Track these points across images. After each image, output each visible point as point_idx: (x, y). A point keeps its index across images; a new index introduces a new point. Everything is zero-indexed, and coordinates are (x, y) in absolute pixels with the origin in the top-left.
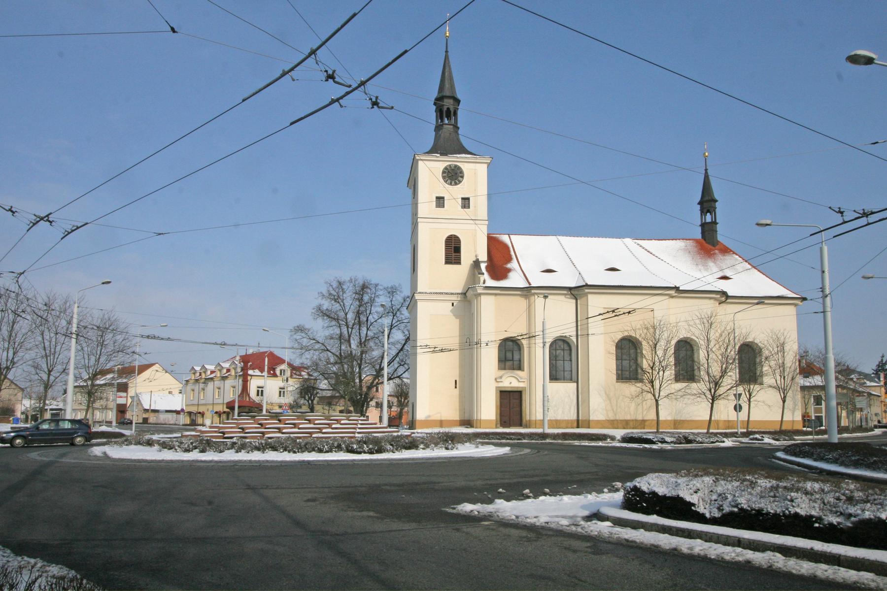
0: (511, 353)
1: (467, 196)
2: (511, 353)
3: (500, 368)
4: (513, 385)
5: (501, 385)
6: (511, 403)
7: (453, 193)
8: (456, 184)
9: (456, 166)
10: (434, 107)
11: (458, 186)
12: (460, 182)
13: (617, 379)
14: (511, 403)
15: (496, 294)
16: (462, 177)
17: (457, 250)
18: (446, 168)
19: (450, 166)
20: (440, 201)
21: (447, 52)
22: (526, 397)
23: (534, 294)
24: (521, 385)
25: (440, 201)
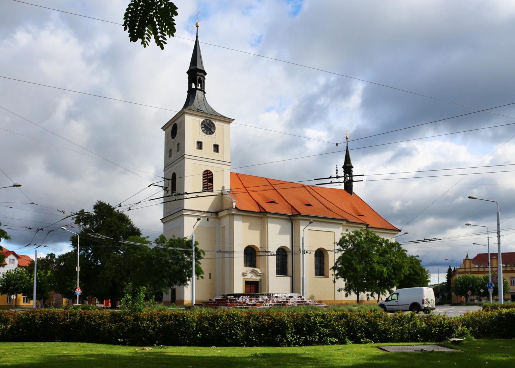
0: (251, 255)
2: (251, 255)
4: (252, 278)
7: (208, 141)
8: (210, 134)
10: (187, 76)
11: (211, 136)
12: (213, 133)
13: (316, 274)
15: (243, 215)
17: (211, 181)
18: (203, 121)
20: (200, 145)
21: (197, 37)
23: (268, 217)
24: (258, 279)
25: (200, 145)
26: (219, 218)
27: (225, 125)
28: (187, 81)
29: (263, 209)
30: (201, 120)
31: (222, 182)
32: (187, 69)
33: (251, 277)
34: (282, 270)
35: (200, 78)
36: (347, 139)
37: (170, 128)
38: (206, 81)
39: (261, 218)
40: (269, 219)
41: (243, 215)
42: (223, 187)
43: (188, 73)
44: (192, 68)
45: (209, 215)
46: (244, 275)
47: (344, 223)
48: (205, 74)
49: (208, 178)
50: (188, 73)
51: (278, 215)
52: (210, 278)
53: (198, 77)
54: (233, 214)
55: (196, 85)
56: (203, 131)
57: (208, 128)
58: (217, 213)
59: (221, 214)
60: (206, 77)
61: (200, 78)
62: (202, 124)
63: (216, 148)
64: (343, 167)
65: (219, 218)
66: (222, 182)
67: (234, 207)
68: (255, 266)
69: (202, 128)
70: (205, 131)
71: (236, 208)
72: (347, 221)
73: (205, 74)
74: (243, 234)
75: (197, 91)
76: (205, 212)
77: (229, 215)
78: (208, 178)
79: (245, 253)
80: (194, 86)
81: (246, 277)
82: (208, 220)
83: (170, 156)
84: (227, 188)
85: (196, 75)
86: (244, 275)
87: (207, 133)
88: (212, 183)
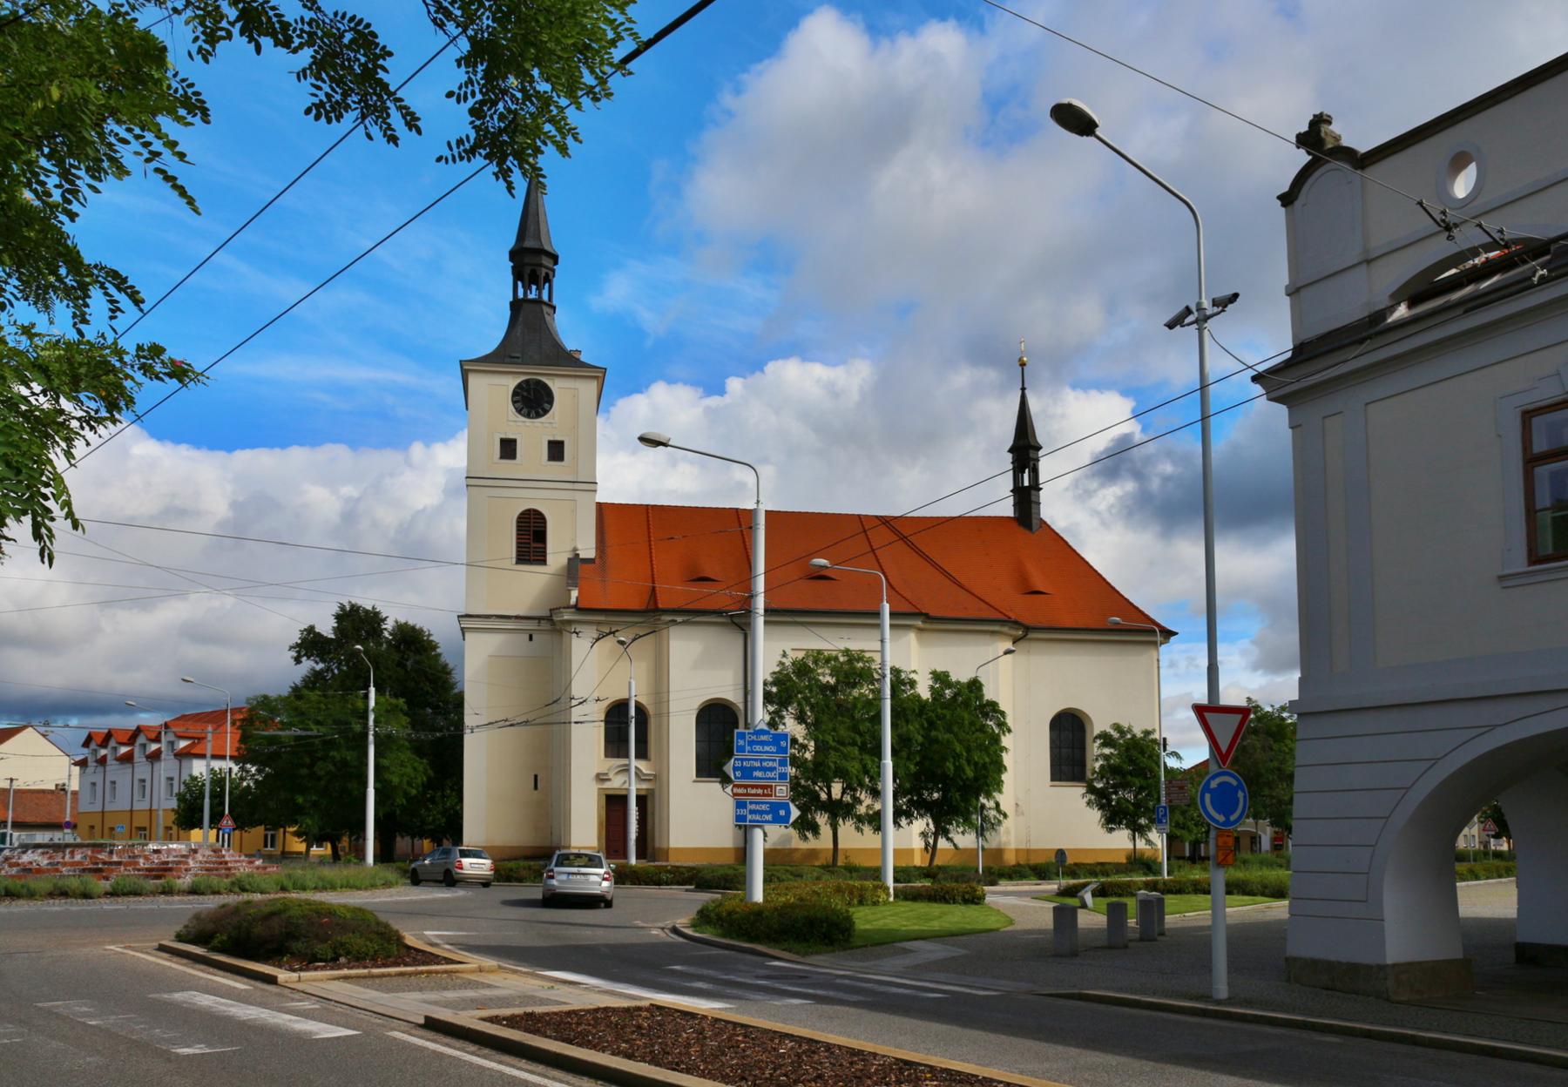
0: (627, 728)
2: (627, 728)
3: (607, 756)
5: (607, 785)
7: (533, 434)
8: (538, 416)
12: (546, 412)
18: (519, 386)
19: (527, 381)
20: (508, 448)
25: (508, 448)
30: (512, 383)
31: (572, 536)
34: (711, 764)
36: (1023, 365)
40: (673, 631)
42: (575, 549)
45: (531, 625)
46: (601, 778)
47: (919, 623)
51: (692, 614)
52: (536, 787)
56: (519, 411)
57: (533, 400)
58: (549, 619)
62: (515, 393)
63: (556, 450)
64: (1010, 451)
66: (572, 536)
67: (573, 601)
69: (514, 403)
71: (575, 606)
72: (927, 617)
74: (597, 670)
75: (525, 305)
76: (517, 617)
79: (607, 721)
81: (607, 785)
82: (531, 638)
84: (588, 550)
86: (601, 778)
87: (528, 416)
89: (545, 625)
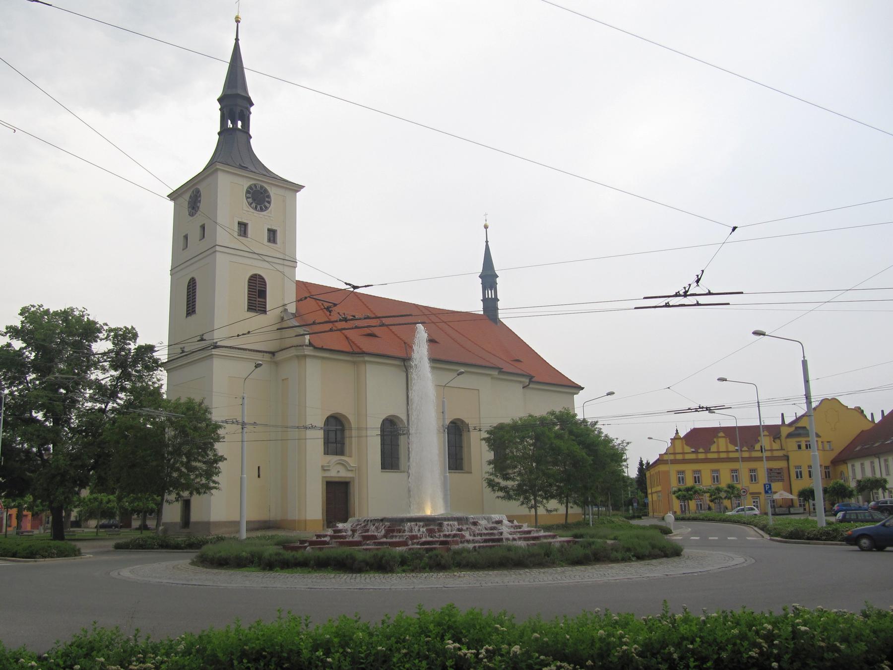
1: (274, 228)
2: (336, 434)
3: (326, 453)
5: (327, 474)
6: (338, 496)
7: (258, 223)
8: (262, 210)
9: (262, 187)
10: (219, 106)
12: (267, 208)
14: (338, 496)
15: (323, 358)
16: (269, 203)
17: (262, 294)
18: (250, 187)
19: (255, 185)
20: (243, 227)
22: (355, 490)
23: (365, 362)
24: (350, 475)
25: (243, 227)
26: (276, 364)
27: (288, 194)
28: (217, 115)
29: (358, 347)
30: (246, 184)
31: (281, 297)
32: (219, 93)
33: (338, 473)
34: (391, 459)
35: (242, 111)
37: (187, 196)
38: (251, 116)
39: (354, 363)
40: (368, 366)
41: (323, 358)
43: (220, 100)
44: (229, 92)
45: (259, 356)
47: (495, 373)
48: (252, 104)
49: (257, 292)
50: (220, 100)
52: (259, 476)
53: (238, 109)
54: (305, 356)
55: (234, 123)
56: (250, 204)
57: (259, 198)
58: (273, 353)
59: (279, 357)
60: (252, 109)
61: (242, 111)
62: (248, 192)
63: (272, 235)
65: (276, 364)
67: (307, 342)
68: (340, 451)
69: (247, 198)
70: (254, 205)
71: (310, 344)
72: (501, 371)
73: (252, 104)
77: (298, 357)
78: (257, 292)
80: (230, 125)
83: (186, 246)
84: (292, 309)
85: (235, 104)
86: (324, 469)
88: (265, 298)
89: (267, 357)
